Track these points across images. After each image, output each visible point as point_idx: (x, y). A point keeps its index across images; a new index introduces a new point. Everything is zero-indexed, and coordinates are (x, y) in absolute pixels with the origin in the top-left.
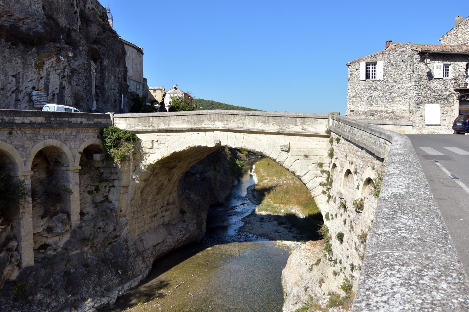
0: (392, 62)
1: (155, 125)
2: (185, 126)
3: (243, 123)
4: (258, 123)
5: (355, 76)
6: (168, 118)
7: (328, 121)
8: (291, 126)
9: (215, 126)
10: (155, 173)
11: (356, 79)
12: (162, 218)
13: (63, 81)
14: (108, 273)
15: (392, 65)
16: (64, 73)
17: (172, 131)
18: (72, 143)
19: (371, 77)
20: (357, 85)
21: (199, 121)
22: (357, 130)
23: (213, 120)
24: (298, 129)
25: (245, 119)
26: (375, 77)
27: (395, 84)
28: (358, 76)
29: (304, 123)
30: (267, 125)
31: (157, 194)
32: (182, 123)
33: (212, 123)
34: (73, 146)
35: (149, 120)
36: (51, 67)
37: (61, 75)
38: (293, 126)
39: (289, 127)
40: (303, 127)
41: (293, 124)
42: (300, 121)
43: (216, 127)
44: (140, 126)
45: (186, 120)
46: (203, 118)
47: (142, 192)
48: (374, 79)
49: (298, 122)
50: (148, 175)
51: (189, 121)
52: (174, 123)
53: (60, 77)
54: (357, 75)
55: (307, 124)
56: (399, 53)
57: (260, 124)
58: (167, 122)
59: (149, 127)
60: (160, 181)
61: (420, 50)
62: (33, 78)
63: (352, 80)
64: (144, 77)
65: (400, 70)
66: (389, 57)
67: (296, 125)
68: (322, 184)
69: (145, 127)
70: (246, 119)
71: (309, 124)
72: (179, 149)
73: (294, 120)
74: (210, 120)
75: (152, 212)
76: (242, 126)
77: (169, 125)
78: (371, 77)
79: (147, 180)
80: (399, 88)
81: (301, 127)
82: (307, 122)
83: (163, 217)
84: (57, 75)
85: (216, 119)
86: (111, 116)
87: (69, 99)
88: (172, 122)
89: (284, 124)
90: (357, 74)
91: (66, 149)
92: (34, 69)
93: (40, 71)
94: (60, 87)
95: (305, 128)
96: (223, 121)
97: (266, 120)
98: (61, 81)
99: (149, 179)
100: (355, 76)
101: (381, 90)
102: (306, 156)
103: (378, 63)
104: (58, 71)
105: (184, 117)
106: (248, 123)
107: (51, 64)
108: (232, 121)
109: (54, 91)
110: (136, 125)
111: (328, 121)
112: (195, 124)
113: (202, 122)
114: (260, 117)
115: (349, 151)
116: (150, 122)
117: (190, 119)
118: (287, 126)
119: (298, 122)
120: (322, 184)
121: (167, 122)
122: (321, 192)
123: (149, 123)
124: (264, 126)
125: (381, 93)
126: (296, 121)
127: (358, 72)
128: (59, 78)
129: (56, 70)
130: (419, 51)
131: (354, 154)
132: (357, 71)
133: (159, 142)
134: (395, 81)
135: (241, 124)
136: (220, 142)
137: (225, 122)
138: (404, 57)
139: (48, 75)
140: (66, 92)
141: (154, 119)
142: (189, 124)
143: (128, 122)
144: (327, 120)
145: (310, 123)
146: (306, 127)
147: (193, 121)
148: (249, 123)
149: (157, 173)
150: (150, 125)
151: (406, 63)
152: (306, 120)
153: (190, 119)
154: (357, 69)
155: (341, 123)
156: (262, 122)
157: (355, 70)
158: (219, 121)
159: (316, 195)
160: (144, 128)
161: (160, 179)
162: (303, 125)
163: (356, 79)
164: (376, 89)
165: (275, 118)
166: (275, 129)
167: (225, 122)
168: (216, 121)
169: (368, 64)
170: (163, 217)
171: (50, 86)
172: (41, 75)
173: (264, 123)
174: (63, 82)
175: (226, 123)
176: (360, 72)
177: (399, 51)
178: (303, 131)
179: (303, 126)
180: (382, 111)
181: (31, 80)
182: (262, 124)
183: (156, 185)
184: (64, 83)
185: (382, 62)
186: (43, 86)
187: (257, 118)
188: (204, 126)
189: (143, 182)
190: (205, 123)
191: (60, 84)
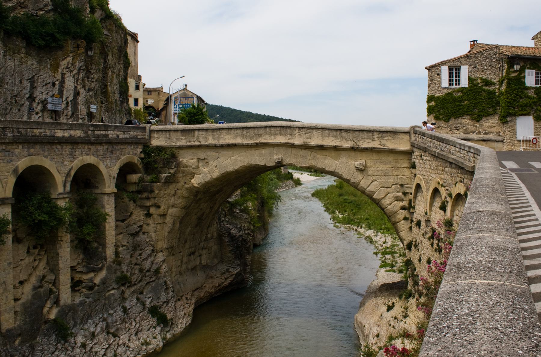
0: (478, 67)
1: (201, 139)
2: (239, 141)
3: (310, 138)
4: (328, 137)
5: (436, 82)
6: (218, 132)
7: (410, 136)
8: (368, 141)
10: (198, 198)
11: (437, 85)
12: (199, 258)
13: (77, 84)
14: (149, 318)
15: (478, 71)
16: (79, 75)
18: (108, 161)
19: (454, 84)
20: (439, 93)
21: (256, 135)
23: (274, 134)
24: (375, 144)
25: (312, 133)
26: (459, 85)
28: (440, 83)
29: (382, 138)
30: (339, 140)
31: (196, 226)
32: (236, 137)
34: (109, 165)
36: (67, 68)
37: (76, 77)
38: (370, 141)
39: (365, 143)
40: (380, 142)
41: (369, 139)
42: (377, 136)
43: (277, 143)
44: (183, 141)
45: (241, 134)
46: (262, 131)
47: (181, 223)
48: (458, 86)
49: (375, 136)
50: (190, 202)
51: (244, 135)
52: (225, 137)
53: (74, 80)
54: (438, 81)
55: (386, 138)
56: (486, 57)
58: (217, 136)
59: (194, 142)
60: (201, 209)
61: (509, 55)
62: (48, 82)
63: (433, 88)
64: (139, 74)
66: (474, 62)
67: (373, 140)
68: (403, 208)
69: (190, 142)
70: (314, 133)
71: (388, 139)
72: (230, 169)
73: (370, 134)
74: (270, 134)
75: (189, 249)
76: (309, 140)
78: (454, 84)
79: (188, 208)
81: (379, 143)
82: (385, 137)
83: (199, 256)
84: (71, 78)
85: (278, 132)
86: (147, 128)
87: (83, 107)
88: (222, 136)
89: (358, 139)
90: (438, 80)
91: (102, 167)
92: (49, 71)
93: (55, 73)
94: (74, 93)
95: (383, 143)
96: (286, 135)
97: (338, 134)
98: (76, 85)
99: (190, 206)
100: (436, 82)
103: (463, 67)
104: (74, 73)
105: (238, 131)
106: (316, 137)
107: (66, 65)
108: (296, 135)
109: (68, 97)
110: (177, 140)
111: (410, 136)
112: (251, 138)
113: (260, 135)
114: (330, 131)
115: (436, 168)
116: (196, 136)
118: (363, 142)
119: (375, 136)
121: (217, 136)
123: (194, 136)
124: (336, 141)
126: (373, 136)
127: (439, 78)
128: (73, 81)
129: (71, 72)
130: (508, 56)
131: (443, 171)
132: (438, 76)
133: (206, 161)
135: (307, 138)
136: (282, 159)
137: (289, 137)
138: (492, 61)
139: (63, 78)
140: (80, 98)
141: (201, 133)
142: (243, 138)
143: (168, 136)
144: (408, 134)
145: (390, 138)
146: (384, 142)
147: (249, 135)
148: (318, 137)
149: (200, 199)
150: (195, 139)
151: (494, 68)
152: (384, 135)
154: (438, 74)
155: (425, 138)
156: (332, 136)
157: (436, 75)
158: (281, 135)
159: (397, 221)
160: (189, 144)
161: (201, 207)
162: (381, 141)
163: (437, 85)
165: (349, 131)
166: (349, 144)
167: (289, 136)
168: (277, 134)
169: (450, 69)
170: (199, 256)
171: (65, 92)
172: (56, 77)
173: (336, 137)
174: (78, 86)
175: (289, 137)
176: (442, 78)
177: (485, 54)
178: (381, 147)
179: (381, 141)
181: (46, 85)
182: (333, 138)
183: (196, 215)
184: (79, 87)
186: (57, 92)
187: (327, 131)
188: (263, 141)
189: (183, 210)
190: (263, 137)
191: (74, 89)
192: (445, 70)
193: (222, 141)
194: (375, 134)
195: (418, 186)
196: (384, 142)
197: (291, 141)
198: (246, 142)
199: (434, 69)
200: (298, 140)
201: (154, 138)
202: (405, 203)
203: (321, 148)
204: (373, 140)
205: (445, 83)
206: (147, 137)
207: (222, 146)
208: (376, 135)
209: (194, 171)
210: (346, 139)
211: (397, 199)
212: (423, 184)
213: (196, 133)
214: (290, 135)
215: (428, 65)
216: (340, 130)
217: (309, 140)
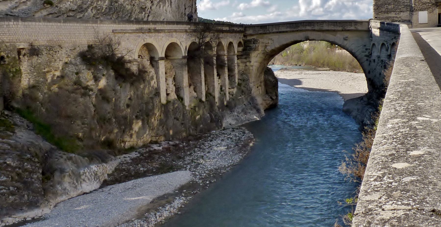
1: (270, 30)
3: (322, 27)
8: (349, 26)
9: (306, 29)
17: (280, 32)
24: (353, 28)
25: (323, 24)
29: (356, 25)
35: (267, 27)
57: (332, 26)
68: (366, 56)
80: (403, 3)
96: (311, 26)
101: (393, 4)
110: (259, 31)
112: (294, 28)
113: (299, 27)
120: (366, 56)
122: (366, 60)
137: (312, 27)
141: (270, 27)
145: (359, 25)
146: (357, 27)
158: (309, 26)
166: (340, 28)
168: (306, 26)
173: (334, 25)
180: (394, 17)
187: (330, 23)
188: (300, 29)
193: (280, 30)
194: (353, 23)
195: (374, 44)
196: (357, 27)
197: (314, 28)
198: (292, 30)
200: (316, 28)
202: (367, 53)
203: (328, 31)
204: (352, 26)
207: (280, 32)
208: (353, 24)
209: (267, 45)
210: (339, 26)
211: (363, 52)
212: (376, 43)
213: (268, 27)
214: (313, 25)
216: (337, 22)
217: (322, 28)
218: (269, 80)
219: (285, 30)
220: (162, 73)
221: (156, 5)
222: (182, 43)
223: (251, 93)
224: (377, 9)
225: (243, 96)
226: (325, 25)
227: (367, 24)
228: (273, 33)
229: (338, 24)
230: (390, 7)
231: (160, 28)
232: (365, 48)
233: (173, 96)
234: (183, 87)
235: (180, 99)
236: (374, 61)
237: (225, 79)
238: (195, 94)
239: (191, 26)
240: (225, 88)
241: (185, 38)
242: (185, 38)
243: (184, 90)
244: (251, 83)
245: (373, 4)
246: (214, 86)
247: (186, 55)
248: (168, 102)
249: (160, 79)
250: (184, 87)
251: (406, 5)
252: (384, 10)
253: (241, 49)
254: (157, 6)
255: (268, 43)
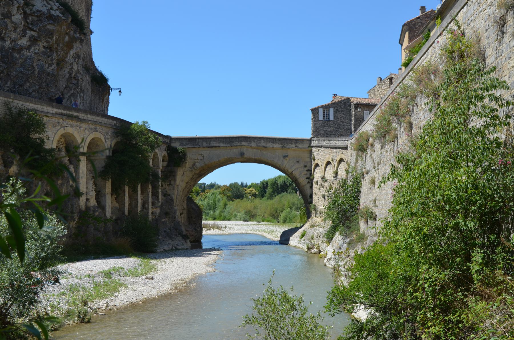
1: (200, 144)
3: (260, 143)
17: (212, 147)
22: (332, 141)
27: (341, 123)
29: (297, 143)
32: (220, 143)
33: (240, 143)
35: (196, 140)
65: (344, 114)
77: (209, 144)
80: (343, 126)
101: (333, 127)
102: (298, 162)
112: (228, 143)
113: (233, 142)
117: (225, 140)
122: (307, 183)
125: (333, 129)
134: (341, 121)
137: (249, 142)
141: (200, 140)
146: (297, 145)
153: (225, 140)
154: (317, 113)
164: (329, 126)
173: (273, 143)
185: (333, 109)
192: (321, 111)
193: (212, 145)
199: (315, 111)
201: (173, 143)
204: (292, 144)
205: (321, 118)
206: (169, 142)
207: (212, 147)
209: (196, 161)
214: (249, 141)
215: (312, 108)
218: (193, 208)
219: (217, 145)
220: (83, 172)
221: (67, 99)
222: (107, 140)
223: (175, 217)
224: (316, 131)
225: (167, 219)
226: (262, 141)
227: (308, 142)
228: (204, 147)
229: (277, 141)
230: (329, 130)
231: (82, 118)
232: (306, 169)
233: (93, 202)
234: (105, 194)
235: (101, 205)
236: (317, 182)
237: (149, 195)
238: (117, 205)
239: (117, 122)
240: (148, 206)
241: (110, 135)
242: (110, 135)
243: (105, 197)
244: (175, 206)
245: (312, 125)
246: (137, 199)
247: (111, 154)
248: (87, 208)
249: (80, 179)
250: (106, 193)
251: (347, 129)
252: (323, 132)
253: (165, 164)
254: (67, 100)
255: (198, 159)
